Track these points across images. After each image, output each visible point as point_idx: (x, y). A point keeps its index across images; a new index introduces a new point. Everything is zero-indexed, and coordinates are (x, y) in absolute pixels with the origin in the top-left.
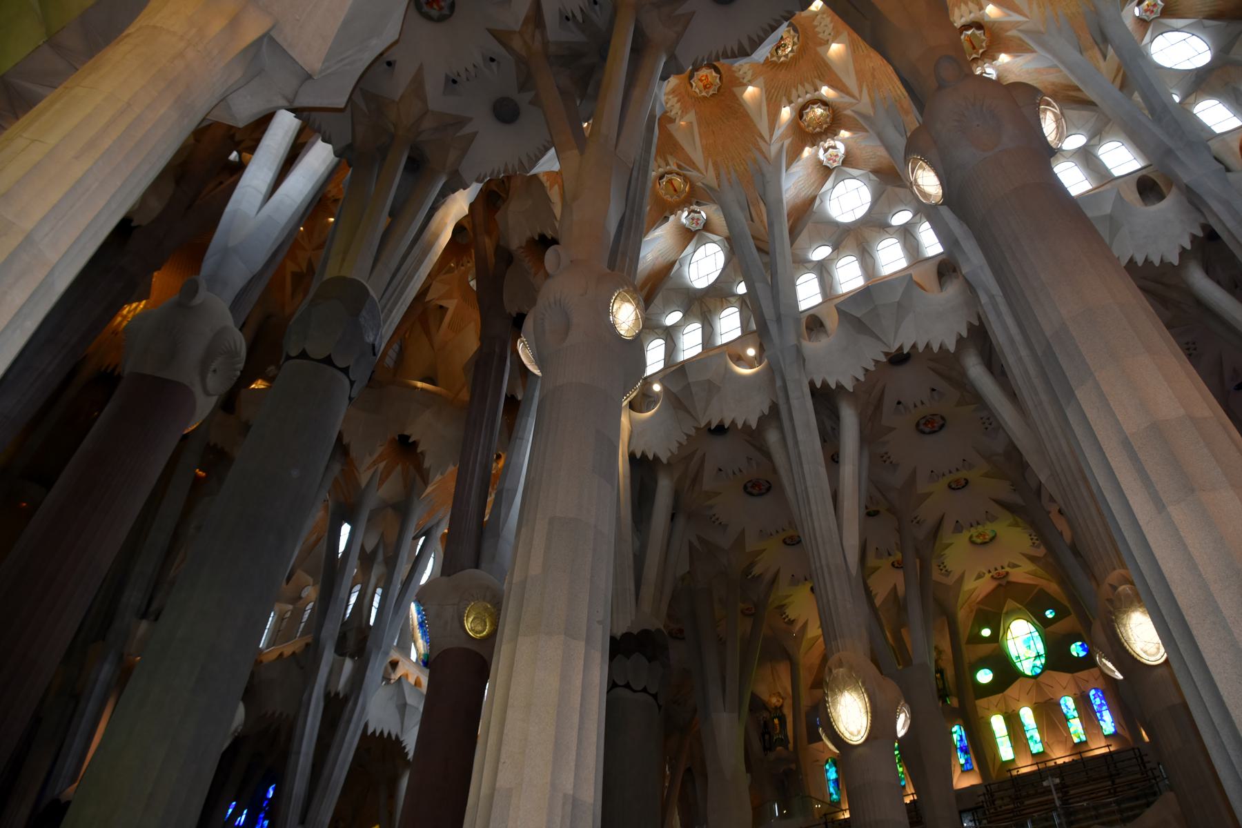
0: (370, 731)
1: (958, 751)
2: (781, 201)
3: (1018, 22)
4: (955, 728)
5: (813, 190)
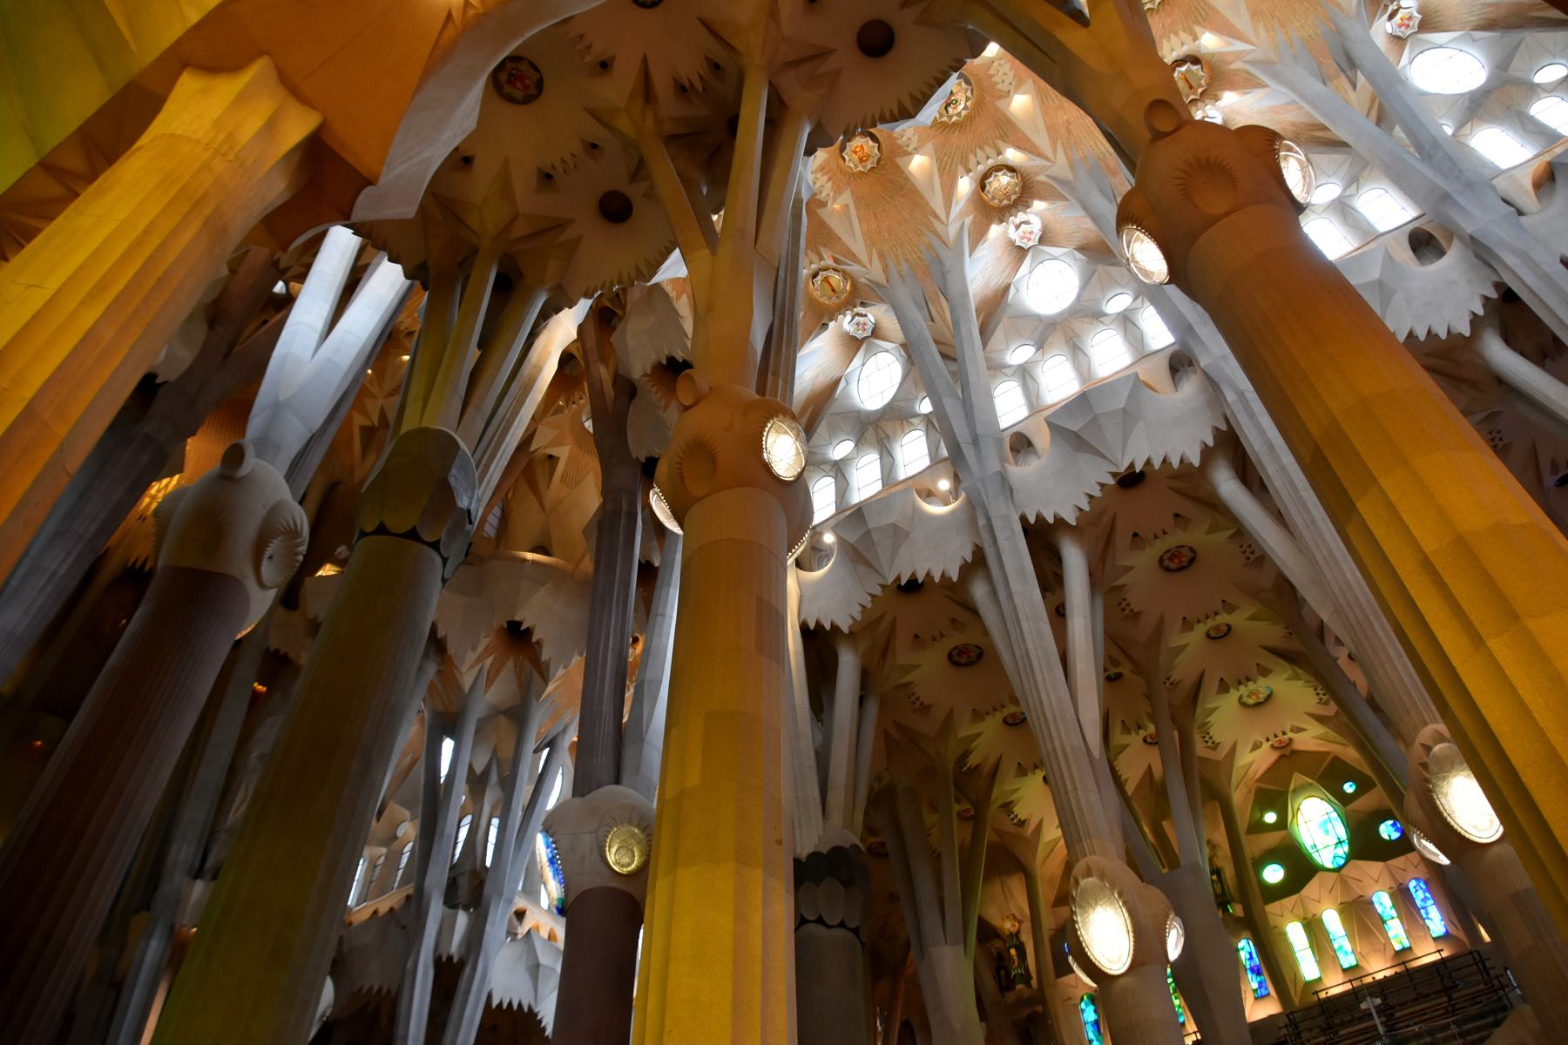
0: (495, 1003)
1: (1249, 972)
2: (965, 294)
3: (1244, 51)
4: (1243, 944)
5: (1006, 277)
